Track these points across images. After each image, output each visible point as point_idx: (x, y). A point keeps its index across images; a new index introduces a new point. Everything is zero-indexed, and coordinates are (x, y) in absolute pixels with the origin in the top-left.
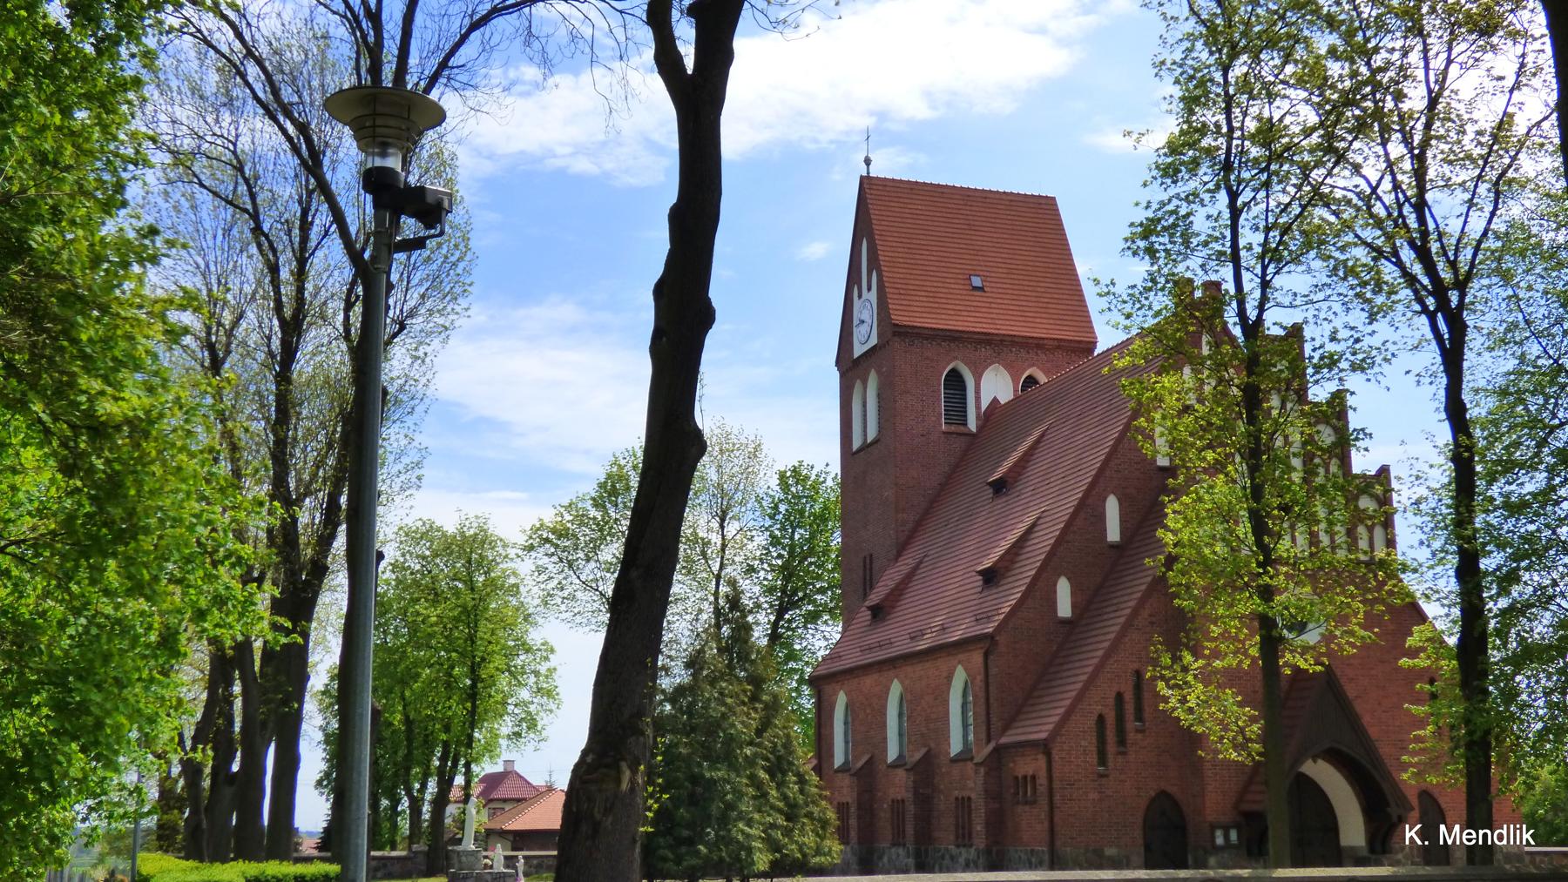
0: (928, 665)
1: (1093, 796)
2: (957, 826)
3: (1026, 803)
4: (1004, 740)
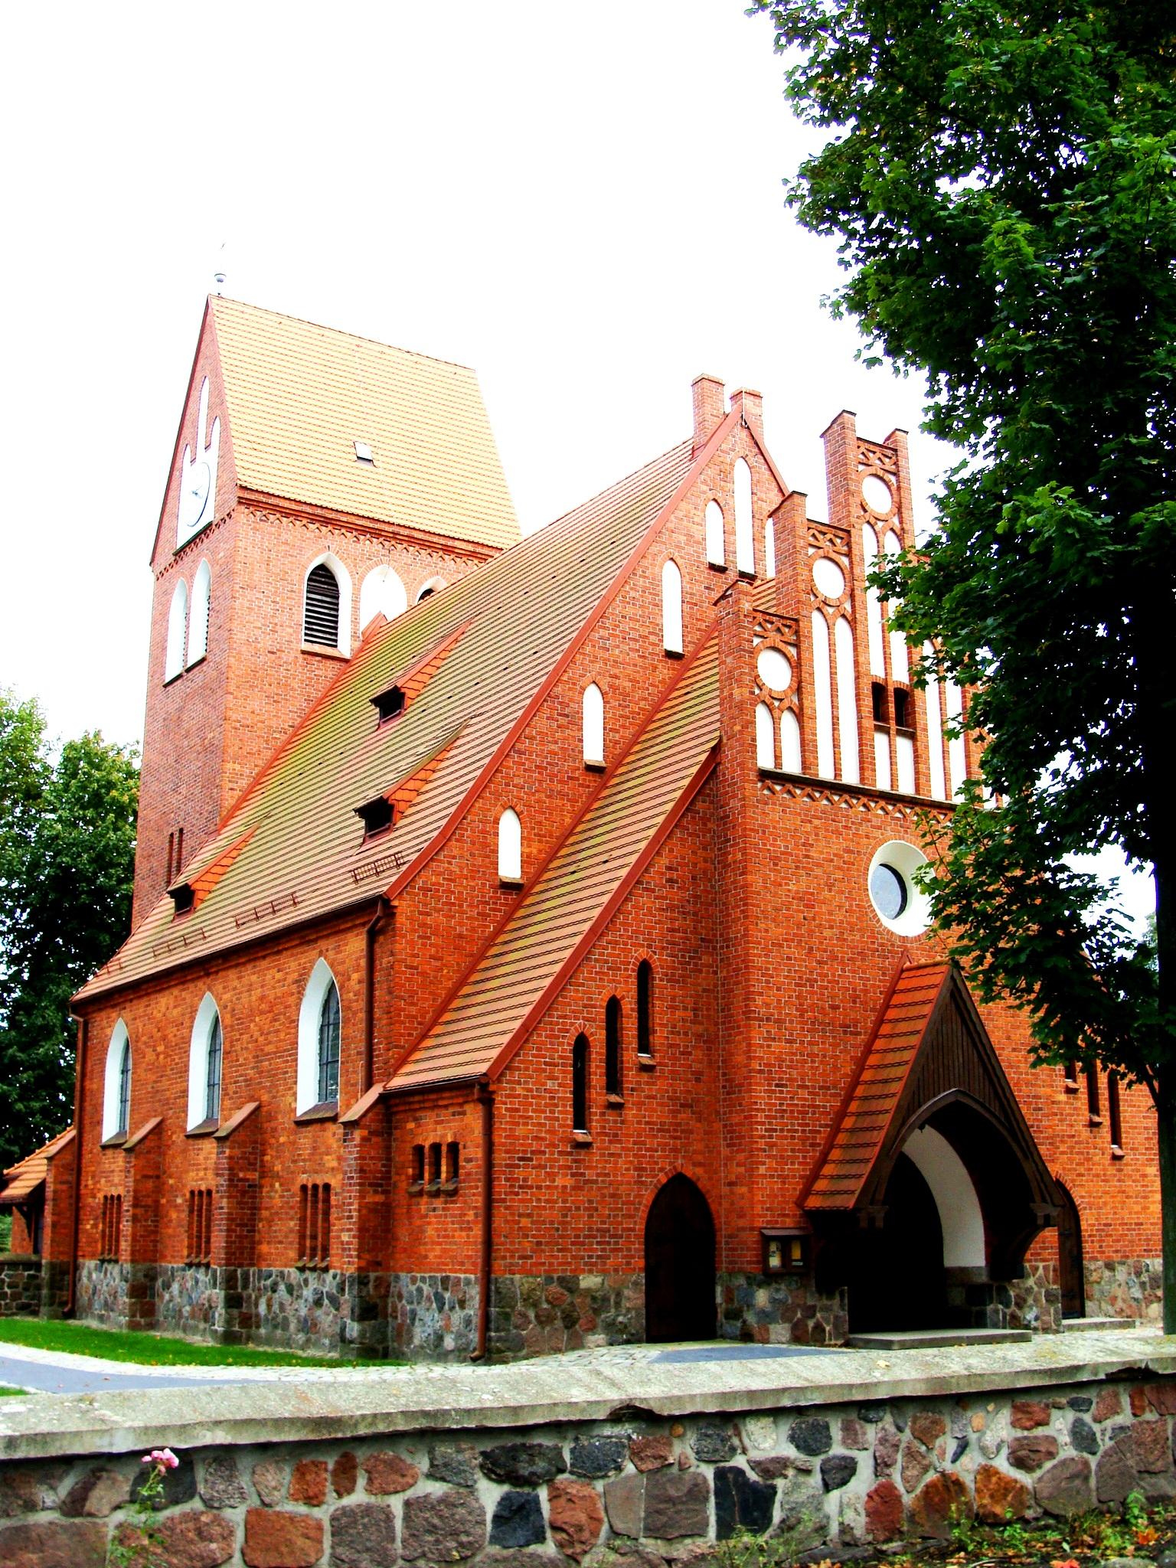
0: (264, 964)
1: (569, 1182)
2: (302, 1237)
3: (436, 1194)
4: (398, 1082)
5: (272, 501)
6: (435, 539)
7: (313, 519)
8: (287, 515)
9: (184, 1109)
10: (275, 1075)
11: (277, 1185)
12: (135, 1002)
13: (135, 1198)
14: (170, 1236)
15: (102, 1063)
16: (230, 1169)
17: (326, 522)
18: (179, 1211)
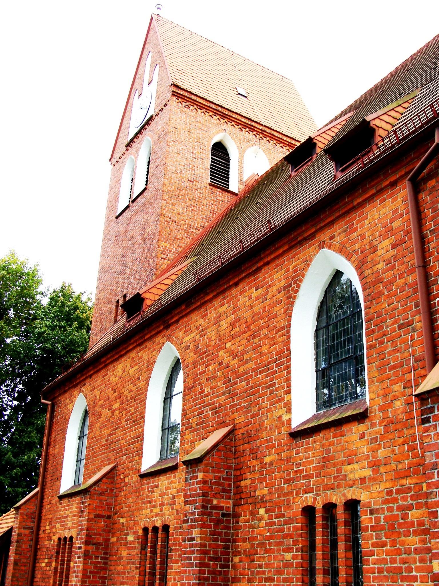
0: (234, 292)
5: (193, 97)
6: (285, 138)
7: (216, 113)
8: (201, 108)
9: (139, 453)
10: (253, 393)
11: (262, 511)
12: (94, 377)
13: (88, 536)
14: (119, 574)
15: (64, 431)
16: (204, 495)
17: (224, 116)
18: (129, 548)
